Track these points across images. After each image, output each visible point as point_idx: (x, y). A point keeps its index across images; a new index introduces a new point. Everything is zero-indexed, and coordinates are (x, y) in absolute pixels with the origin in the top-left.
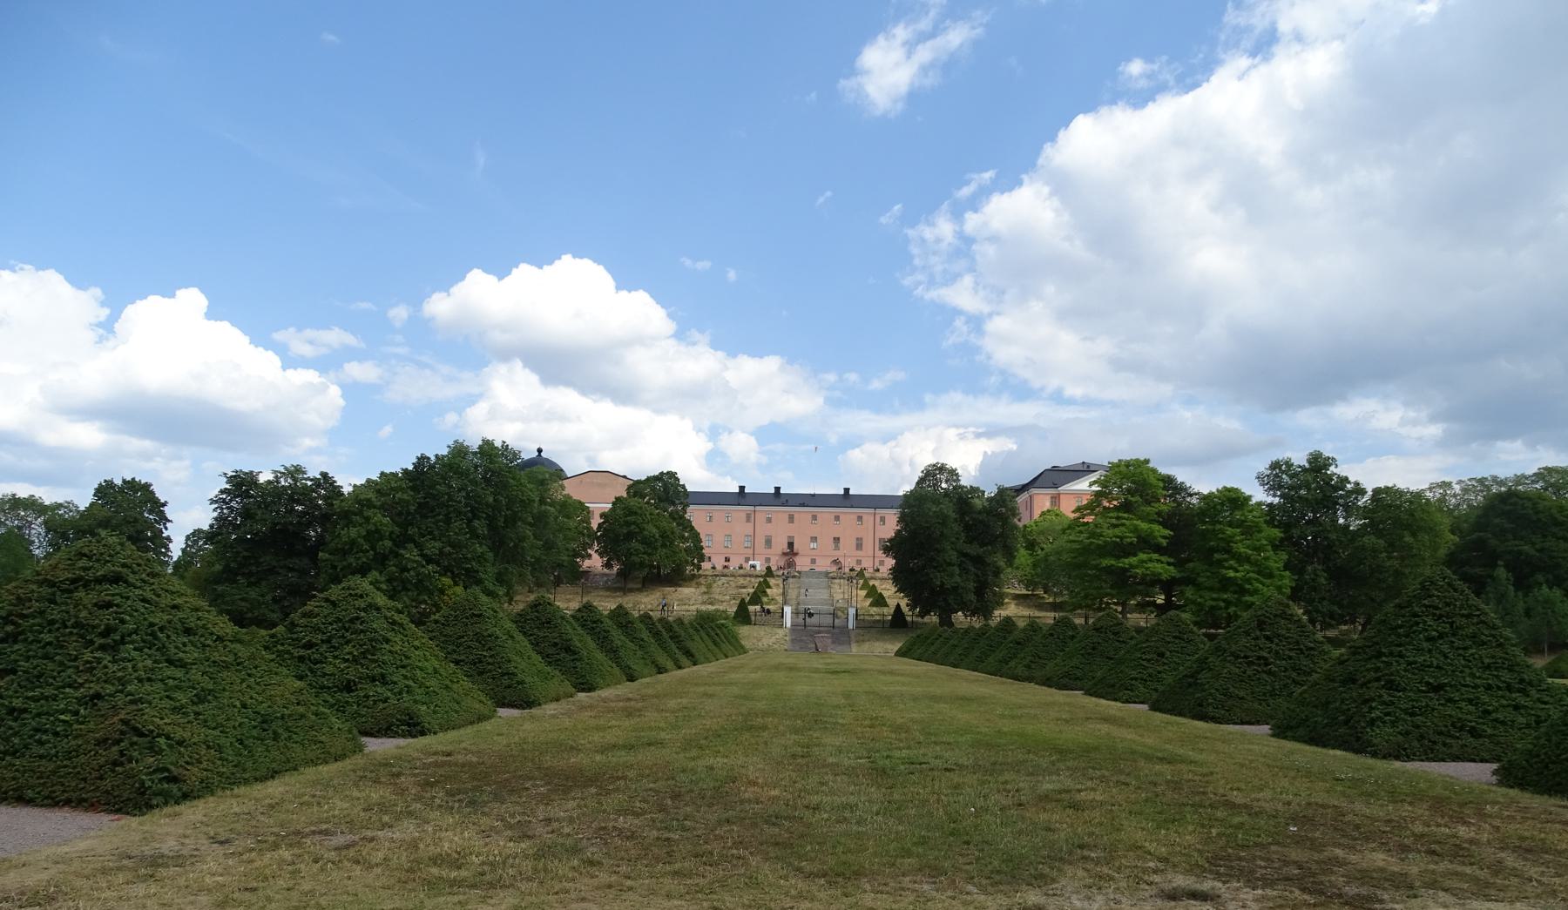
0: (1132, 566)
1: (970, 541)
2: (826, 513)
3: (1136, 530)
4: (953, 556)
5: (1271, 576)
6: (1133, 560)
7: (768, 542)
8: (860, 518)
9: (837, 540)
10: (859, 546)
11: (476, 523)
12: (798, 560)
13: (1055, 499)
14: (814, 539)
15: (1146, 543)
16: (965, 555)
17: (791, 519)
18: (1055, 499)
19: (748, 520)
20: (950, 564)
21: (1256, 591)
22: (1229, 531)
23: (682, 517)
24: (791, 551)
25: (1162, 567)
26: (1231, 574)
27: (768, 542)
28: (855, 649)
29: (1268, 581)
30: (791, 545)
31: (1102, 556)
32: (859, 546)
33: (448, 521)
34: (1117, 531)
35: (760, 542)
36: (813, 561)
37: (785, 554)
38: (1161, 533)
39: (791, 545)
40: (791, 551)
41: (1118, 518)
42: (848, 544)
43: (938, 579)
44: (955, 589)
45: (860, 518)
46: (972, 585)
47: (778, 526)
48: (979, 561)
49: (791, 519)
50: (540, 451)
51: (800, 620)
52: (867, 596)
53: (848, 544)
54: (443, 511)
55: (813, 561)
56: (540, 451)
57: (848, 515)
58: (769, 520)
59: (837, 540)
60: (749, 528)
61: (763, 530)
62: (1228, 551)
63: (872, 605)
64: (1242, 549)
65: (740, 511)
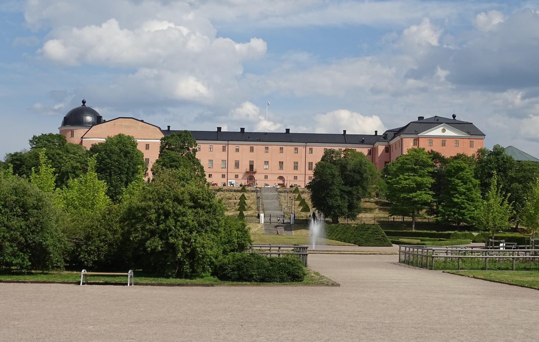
0: (413, 197)
1: (346, 184)
2: (274, 147)
3: (415, 181)
4: (338, 192)
5: (473, 201)
6: (414, 194)
7: (237, 165)
8: (296, 149)
9: (281, 163)
10: (296, 168)
11: (122, 176)
12: (256, 176)
13: (416, 141)
14: (267, 163)
15: (420, 186)
16: (344, 191)
17: (252, 150)
18: (416, 141)
19: (224, 150)
20: (335, 196)
21: (465, 208)
22: (457, 181)
23: (194, 158)
24: (251, 173)
25: (427, 196)
26: (456, 200)
27: (237, 165)
28: (293, 232)
29: (471, 203)
30: (251, 167)
31: (402, 192)
32: (296, 168)
33: (110, 175)
34: (407, 182)
35: (232, 164)
36: (266, 177)
37: (247, 172)
38: (429, 181)
39: (251, 167)
40: (251, 173)
41: (409, 176)
43: (330, 202)
44: (339, 206)
45: (296, 149)
46: (346, 204)
47: (243, 153)
48: (350, 193)
49: (252, 150)
50: (84, 102)
51: (268, 219)
52: (300, 205)
54: (108, 171)
55: (266, 177)
56: (84, 102)
58: (237, 150)
59: (281, 163)
60: (224, 156)
61: (233, 156)
62: (456, 190)
63: (302, 211)
64: (462, 189)
65: (218, 146)
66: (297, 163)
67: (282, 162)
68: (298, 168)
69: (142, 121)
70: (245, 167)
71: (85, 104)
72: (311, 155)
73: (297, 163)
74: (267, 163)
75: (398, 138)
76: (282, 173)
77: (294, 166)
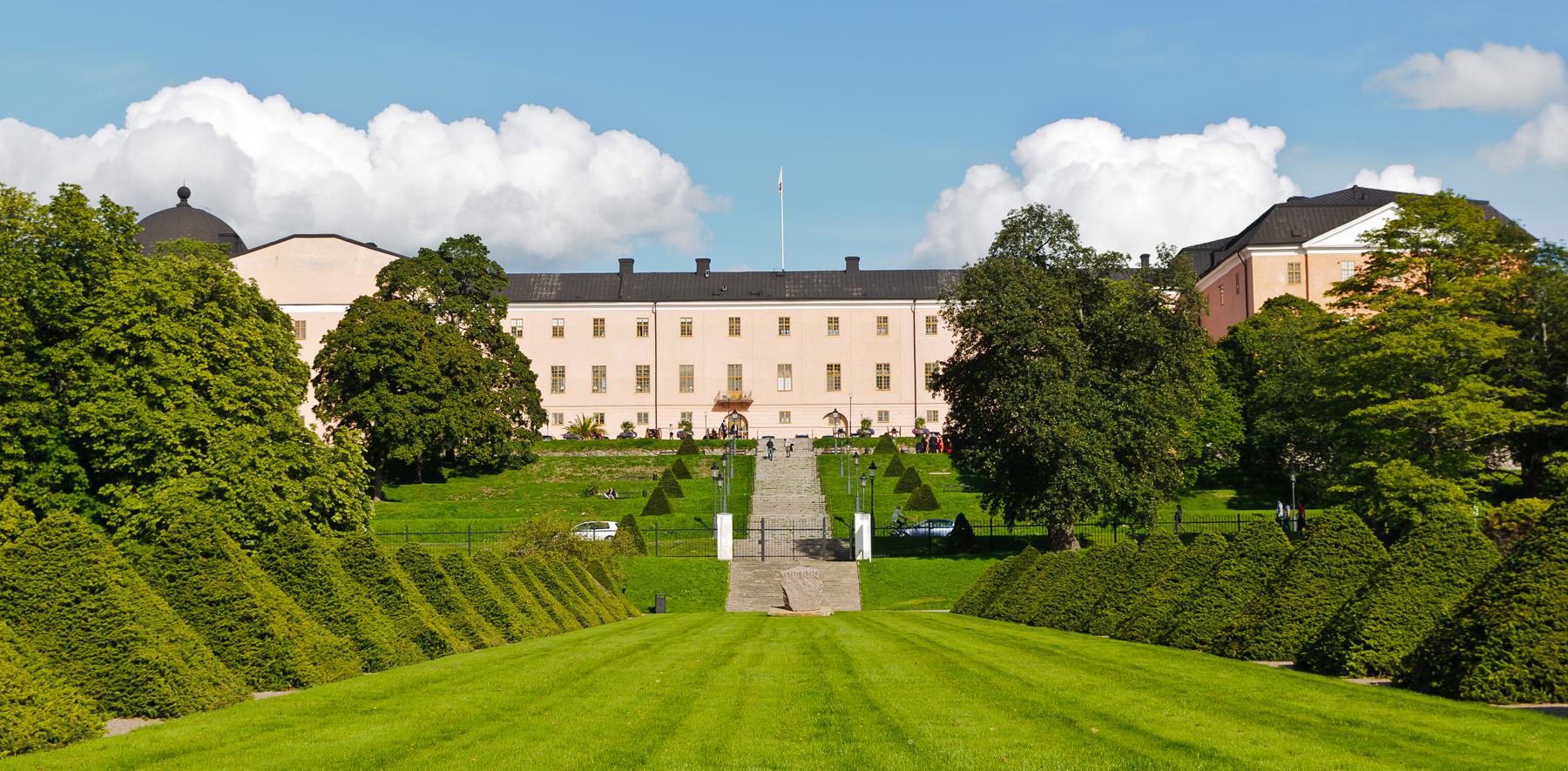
2: (809, 314)
7: (687, 380)
9: (834, 368)
10: (883, 383)
19: (642, 329)
27: (687, 380)
32: (883, 383)
38: (1490, 338)
42: (859, 378)
47: (705, 341)
50: (184, 193)
52: (900, 489)
53: (859, 378)
56: (184, 193)
57: (858, 314)
58: (686, 330)
59: (834, 368)
66: (887, 366)
67: (838, 367)
68: (889, 372)
69: (372, 246)
70: (713, 384)
71: (190, 201)
72: (932, 337)
73: (887, 366)
74: (785, 369)
75: (1231, 264)
76: (837, 400)
77: (879, 379)
